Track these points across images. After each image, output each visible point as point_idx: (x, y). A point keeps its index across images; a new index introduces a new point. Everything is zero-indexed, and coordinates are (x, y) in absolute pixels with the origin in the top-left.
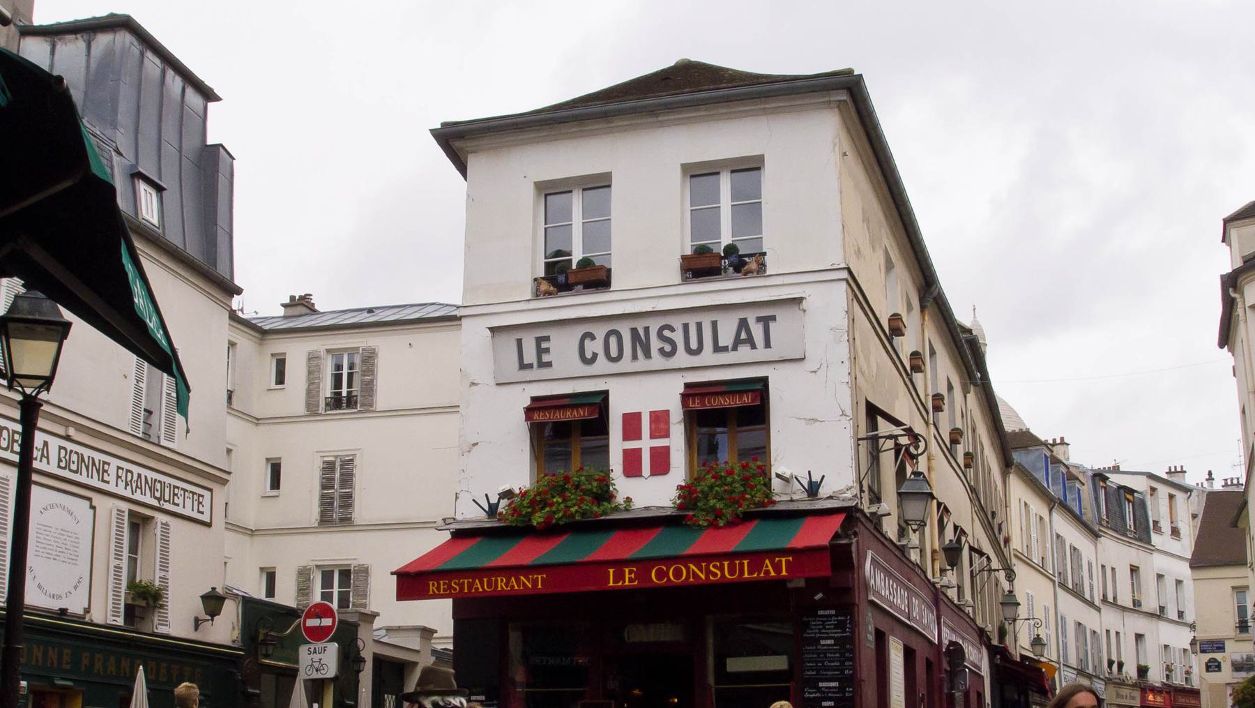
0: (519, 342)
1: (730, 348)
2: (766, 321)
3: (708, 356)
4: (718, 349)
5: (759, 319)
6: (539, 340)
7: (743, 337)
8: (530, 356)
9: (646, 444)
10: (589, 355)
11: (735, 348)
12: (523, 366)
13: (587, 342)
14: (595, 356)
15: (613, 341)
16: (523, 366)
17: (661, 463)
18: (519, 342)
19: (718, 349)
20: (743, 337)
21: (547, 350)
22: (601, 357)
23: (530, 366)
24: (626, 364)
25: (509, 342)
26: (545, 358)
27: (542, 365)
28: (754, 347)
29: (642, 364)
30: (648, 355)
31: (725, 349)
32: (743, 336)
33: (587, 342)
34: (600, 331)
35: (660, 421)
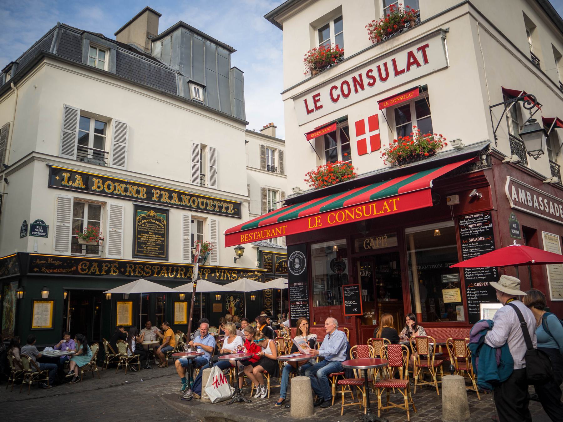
0: (305, 101)
1: (406, 70)
2: (423, 49)
3: (393, 80)
4: (397, 73)
5: (419, 49)
6: (314, 97)
7: (412, 61)
8: (311, 106)
9: (368, 135)
10: (335, 97)
11: (408, 69)
12: (309, 112)
13: (334, 90)
14: (338, 96)
15: (345, 87)
16: (309, 112)
17: (376, 143)
18: (305, 101)
19: (397, 73)
20: (412, 61)
21: (319, 100)
22: (341, 96)
23: (312, 111)
24: (354, 97)
25: (301, 101)
26: (319, 104)
27: (317, 108)
28: (419, 65)
29: (362, 94)
30: (363, 88)
31: (403, 71)
32: (412, 60)
33: (334, 90)
34: (338, 83)
35: (374, 122)
